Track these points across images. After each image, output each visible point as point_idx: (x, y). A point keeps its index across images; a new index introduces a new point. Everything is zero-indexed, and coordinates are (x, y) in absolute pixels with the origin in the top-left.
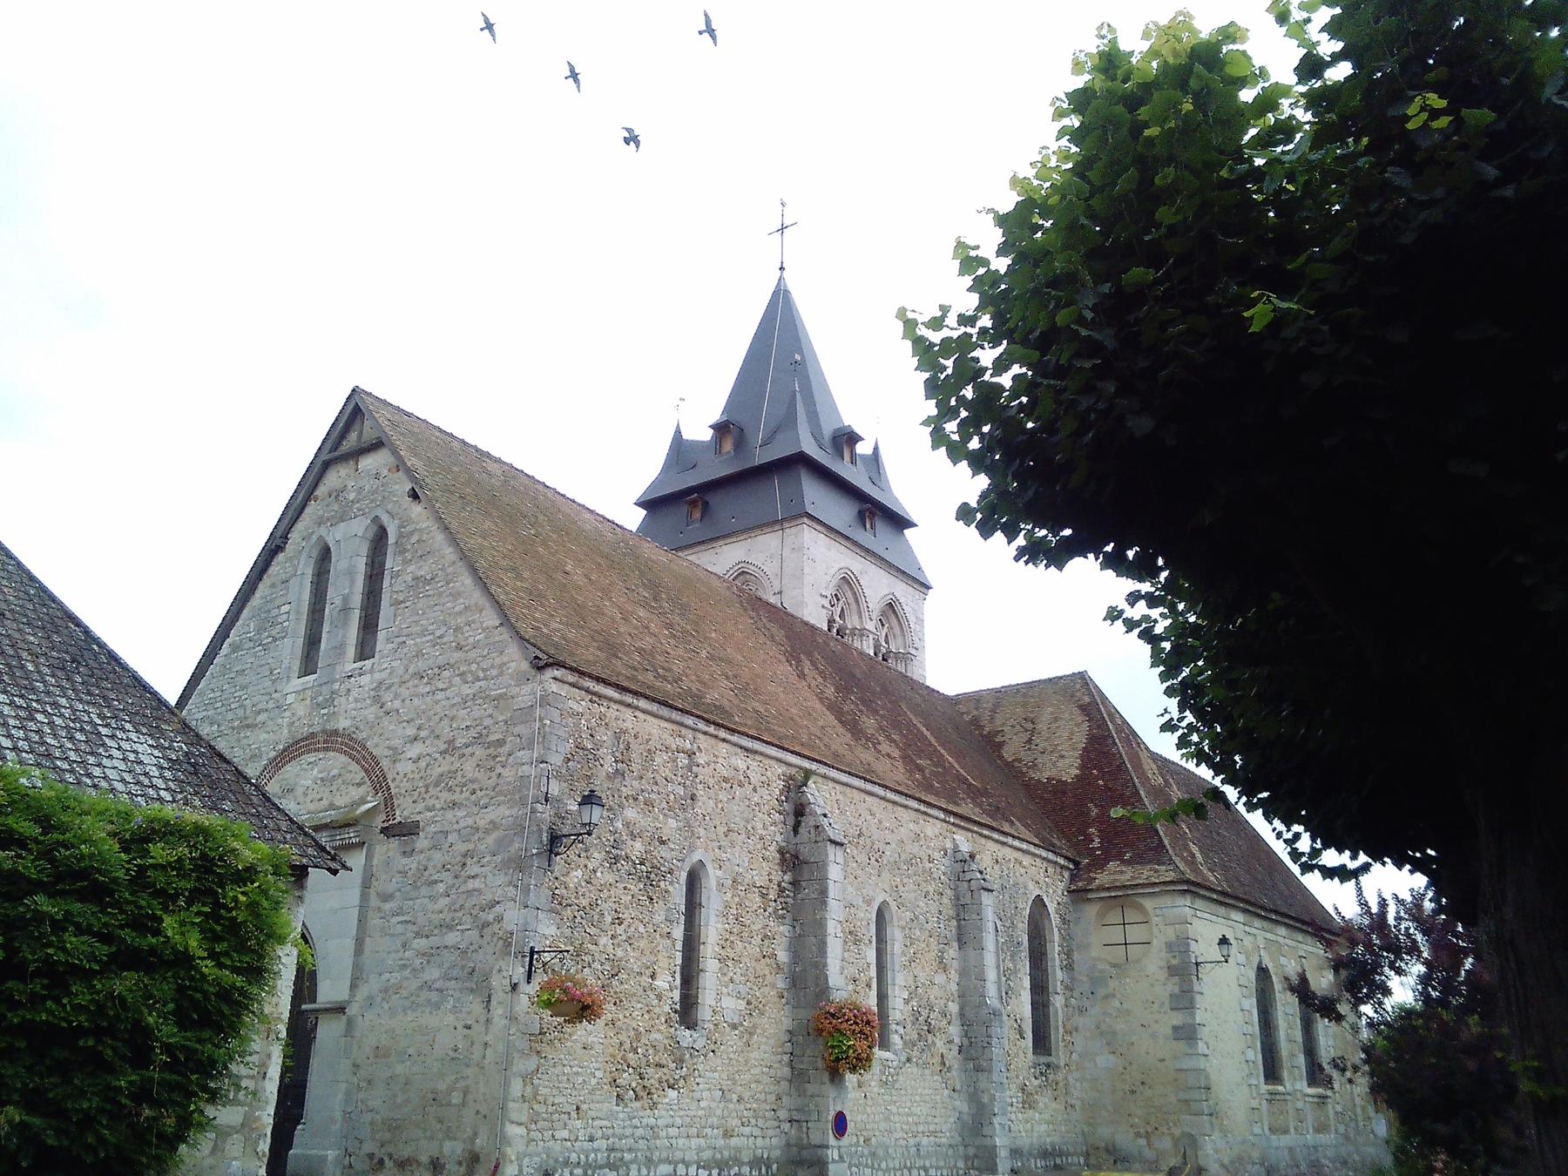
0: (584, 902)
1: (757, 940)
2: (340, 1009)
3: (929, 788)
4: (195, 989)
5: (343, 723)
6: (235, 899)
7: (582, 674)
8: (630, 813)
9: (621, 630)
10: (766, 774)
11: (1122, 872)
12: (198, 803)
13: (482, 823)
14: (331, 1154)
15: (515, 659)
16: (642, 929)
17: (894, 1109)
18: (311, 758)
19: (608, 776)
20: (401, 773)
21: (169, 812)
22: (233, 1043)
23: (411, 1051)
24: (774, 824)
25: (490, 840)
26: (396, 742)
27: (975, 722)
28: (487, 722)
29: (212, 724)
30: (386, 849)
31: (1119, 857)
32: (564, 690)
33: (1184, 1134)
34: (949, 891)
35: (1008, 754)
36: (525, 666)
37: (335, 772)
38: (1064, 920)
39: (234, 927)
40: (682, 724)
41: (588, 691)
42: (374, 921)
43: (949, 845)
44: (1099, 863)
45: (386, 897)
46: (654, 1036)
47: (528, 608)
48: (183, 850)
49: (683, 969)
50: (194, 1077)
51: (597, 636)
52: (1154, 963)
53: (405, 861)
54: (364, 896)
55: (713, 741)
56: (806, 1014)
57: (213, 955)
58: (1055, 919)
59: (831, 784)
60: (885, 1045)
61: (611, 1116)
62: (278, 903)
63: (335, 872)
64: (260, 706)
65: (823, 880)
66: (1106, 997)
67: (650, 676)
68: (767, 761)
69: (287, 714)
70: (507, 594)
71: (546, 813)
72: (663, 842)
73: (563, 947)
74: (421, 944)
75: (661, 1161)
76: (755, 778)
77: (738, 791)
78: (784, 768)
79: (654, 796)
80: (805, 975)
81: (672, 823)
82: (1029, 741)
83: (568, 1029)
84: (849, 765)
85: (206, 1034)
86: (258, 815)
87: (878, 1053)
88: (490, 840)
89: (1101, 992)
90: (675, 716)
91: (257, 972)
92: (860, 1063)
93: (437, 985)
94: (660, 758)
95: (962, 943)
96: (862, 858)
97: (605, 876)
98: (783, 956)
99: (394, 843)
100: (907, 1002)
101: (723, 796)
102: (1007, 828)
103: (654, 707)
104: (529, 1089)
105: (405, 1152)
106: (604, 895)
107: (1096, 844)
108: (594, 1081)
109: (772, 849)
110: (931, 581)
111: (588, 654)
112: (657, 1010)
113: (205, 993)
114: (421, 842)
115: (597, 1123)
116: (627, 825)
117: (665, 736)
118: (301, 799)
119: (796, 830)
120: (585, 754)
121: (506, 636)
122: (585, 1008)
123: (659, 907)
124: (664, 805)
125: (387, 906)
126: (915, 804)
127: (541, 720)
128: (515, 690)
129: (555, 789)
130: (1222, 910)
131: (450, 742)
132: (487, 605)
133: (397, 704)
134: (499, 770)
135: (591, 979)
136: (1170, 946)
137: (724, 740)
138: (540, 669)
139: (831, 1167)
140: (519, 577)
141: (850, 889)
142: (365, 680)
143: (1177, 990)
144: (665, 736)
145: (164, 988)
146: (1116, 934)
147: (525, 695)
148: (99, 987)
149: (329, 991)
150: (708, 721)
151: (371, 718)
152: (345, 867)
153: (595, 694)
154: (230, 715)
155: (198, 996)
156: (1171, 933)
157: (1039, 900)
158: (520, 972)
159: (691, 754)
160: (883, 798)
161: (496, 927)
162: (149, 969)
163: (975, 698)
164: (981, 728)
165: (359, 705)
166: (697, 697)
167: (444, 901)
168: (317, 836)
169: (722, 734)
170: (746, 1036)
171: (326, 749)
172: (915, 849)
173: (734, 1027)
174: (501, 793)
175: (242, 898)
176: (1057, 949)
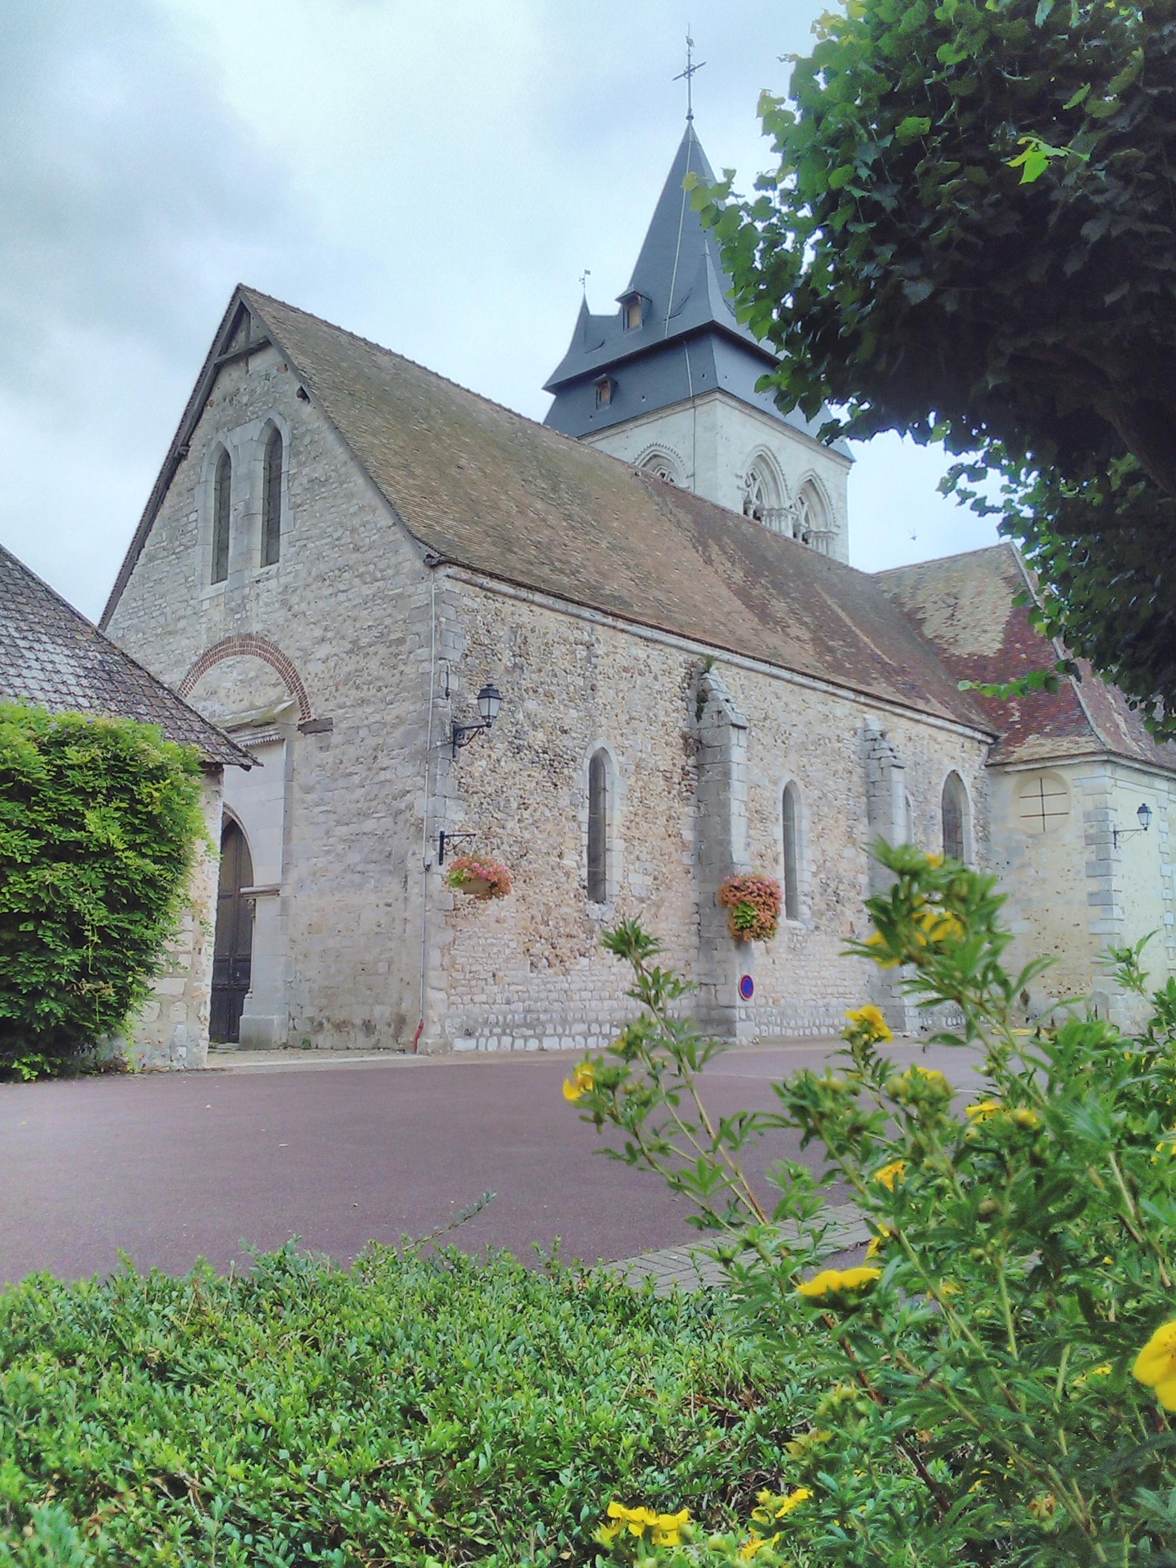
0: (490, 790)
1: (662, 821)
2: (274, 892)
3: (838, 668)
4: (122, 877)
5: (255, 627)
6: (151, 796)
7: (475, 570)
8: (531, 705)
9: (517, 524)
10: (668, 662)
11: (1042, 745)
12: (113, 708)
13: (388, 718)
14: (276, 1018)
15: (410, 559)
16: (548, 813)
17: (802, 973)
18: (229, 661)
19: (507, 670)
20: (312, 672)
21: (82, 718)
22: (163, 924)
23: (340, 927)
24: (677, 710)
25: (398, 733)
26: (306, 643)
27: (896, 600)
28: (388, 621)
29: (137, 632)
30: (305, 745)
31: (1039, 731)
32: (458, 587)
33: (1095, 993)
34: (859, 770)
35: (929, 631)
36: (419, 565)
37: (252, 674)
38: (981, 794)
39: (152, 821)
40: (578, 617)
41: (481, 587)
42: (299, 812)
43: (859, 724)
44: (1018, 737)
45: (308, 790)
46: (565, 910)
47: (419, 505)
48: (96, 751)
49: (589, 847)
50: (129, 953)
51: (491, 531)
52: (1072, 833)
53: (323, 755)
54: (288, 789)
55: (612, 632)
56: (713, 888)
57: (132, 846)
58: (971, 793)
59: (735, 670)
60: (792, 913)
61: (526, 981)
62: (191, 798)
63: (248, 768)
64: (181, 613)
65: (726, 762)
66: (1023, 866)
67: (546, 570)
68: (668, 650)
69: (204, 620)
70: (398, 492)
71: (448, 707)
72: (565, 732)
73: (472, 831)
74: (342, 831)
75: (575, 1021)
76: (656, 667)
77: (639, 680)
78: (685, 656)
79: (553, 688)
80: (710, 852)
81: (573, 713)
83: (480, 904)
84: (753, 650)
85: (137, 916)
86: (172, 717)
87: (783, 921)
88: (398, 733)
89: (1016, 862)
90: (572, 608)
91: (176, 860)
92: (764, 931)
93: (358, 869)
94: (558, 651)
95: (871, 818)
96: (768, 740)
97: (508, 765)
98: (688, 835)
99: (311, 738)
100: (815, 874)
101: (623, 686)
102: (920, 705)
103: (550, 601)
104: (447, 960)
105: (340, 1016)
106: (509, 782)
107: (1017, 717)
108: (508, 951)
109: (675, 734)
110: (856, 456)
111: (482, 551)
112: (566, 886)
113: (131, 880)
114: (336, 738)
115: (512, 988)
116: (528, 716)
117: (563, 629)
118: (224, 700)
119: (699, 716)
120: (482, 649)
121: (399, 535)
122: (494, 885)
123: (564, 792)
124: (565, 696)
125: (309, 797)
126: (823, 686)
127: (437, 618)
128: (411, 589)
129: (454, 684)
130: (1145, 779)
131: (354, 642)
132: (380, 505)
133: (304, 606)
134: (401, 667)
135: (499, 860)
136: (1088, 816)
137: (622, 631)
138: (433, 567)
139: (738, 1025)
140: (412, 475)
141: (756, 771)
142: (272, 584)
143: (1093, 858)
144: (563, 629)
145: (92, 876)
146: (1034, 806)
147: (421, 593)
148: (34, 877)
149: (264, 873)
150: (605, 613)
151: (281, 621)
152: (255, 762)
153: (489, 590)
154: (153, 623)
155: (125, 883)
156: (1089, 804)
157: (955, 776)
158: (432, 854)
159: (589, 646)
160: (789, 681)
161: (408, 814)
162: (78, 860)
163: (896, 576)
164: (902, 605)
165: (269, 609)
166: (595, 589)
167: (360, 792)
168: (231, 736)
169: (621, 624)
170: (654, 909)
171: (243, 653)
172: (823, 729)
173: (642, 900)
174: (405, 689)
175: (156, 794)
176: (973, 822)
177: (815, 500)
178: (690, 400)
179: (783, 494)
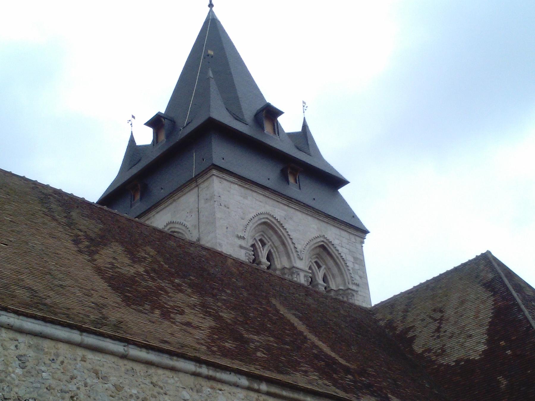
27: (390, 325)
35: (418, 348)
82: (438, 330)
177: (331, 263)
178: (193, 182)
179: (294, 256)
